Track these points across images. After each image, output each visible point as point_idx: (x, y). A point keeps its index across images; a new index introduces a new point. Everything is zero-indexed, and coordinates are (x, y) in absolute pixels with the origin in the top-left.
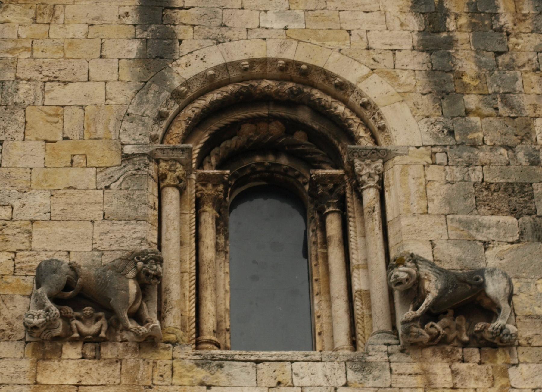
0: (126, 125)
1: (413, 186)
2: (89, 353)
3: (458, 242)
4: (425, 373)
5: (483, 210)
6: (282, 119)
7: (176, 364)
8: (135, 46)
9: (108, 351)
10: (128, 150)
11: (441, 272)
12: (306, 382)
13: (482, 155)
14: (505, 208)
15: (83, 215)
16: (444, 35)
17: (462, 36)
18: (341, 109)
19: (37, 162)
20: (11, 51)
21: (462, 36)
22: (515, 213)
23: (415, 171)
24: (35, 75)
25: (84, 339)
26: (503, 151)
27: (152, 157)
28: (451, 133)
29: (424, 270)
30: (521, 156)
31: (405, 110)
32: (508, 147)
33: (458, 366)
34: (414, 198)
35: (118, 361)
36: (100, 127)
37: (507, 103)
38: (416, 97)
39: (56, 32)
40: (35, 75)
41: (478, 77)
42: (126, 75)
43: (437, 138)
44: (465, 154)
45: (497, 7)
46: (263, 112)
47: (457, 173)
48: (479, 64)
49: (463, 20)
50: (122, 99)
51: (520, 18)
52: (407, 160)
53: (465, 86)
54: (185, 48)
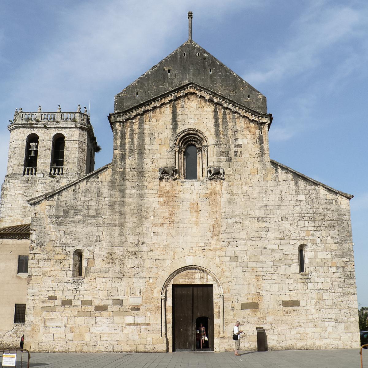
0: (171, 141)
1: (212, 152)
2: (167, 181)
3: (217, 162)
4: (211, 184)
5: (221, 156)
6: (193, 137)
7: (178, 182)
8: (172, 126)
9: (169, 180)
10: (171, 146)
11: (214, 169)
12: (195, 185)
13: (222, 146)
14: (224, 156)
15: (165, 158)
16: (218, 123)
17: (221, 123)
18: (202, 137)
19: (158, 148)
20: (153, 127)
21: (221, 123)
22: (226, 157)
23: (212, 149)
24: (157, 132)
25: (166, 179)
26: (225, 145)
27: (174, 147)
28: (218, 142)
29: (212, 169)
30: (227, 146)
31: (211, 138)
32: (226, 145)
33: (216, 182)
34: (212, 154)
35: (170, 182)
36: (167, 142)
37: (227, 137)
38: (213, 135)
39: (160, 123)
40: (157, 132)
41: (223, 131)
42: (170, 132)
43: (216, 143)
44: (220, 146)
45: (226, 117)
46: (191, 136)
47: (218, 149)
48: (223, 129)
49: (221, 120)
50: (170, 137)
51: (230, 120)
52: (211, 147)
53: (221, 133)
54: (179, 126)
